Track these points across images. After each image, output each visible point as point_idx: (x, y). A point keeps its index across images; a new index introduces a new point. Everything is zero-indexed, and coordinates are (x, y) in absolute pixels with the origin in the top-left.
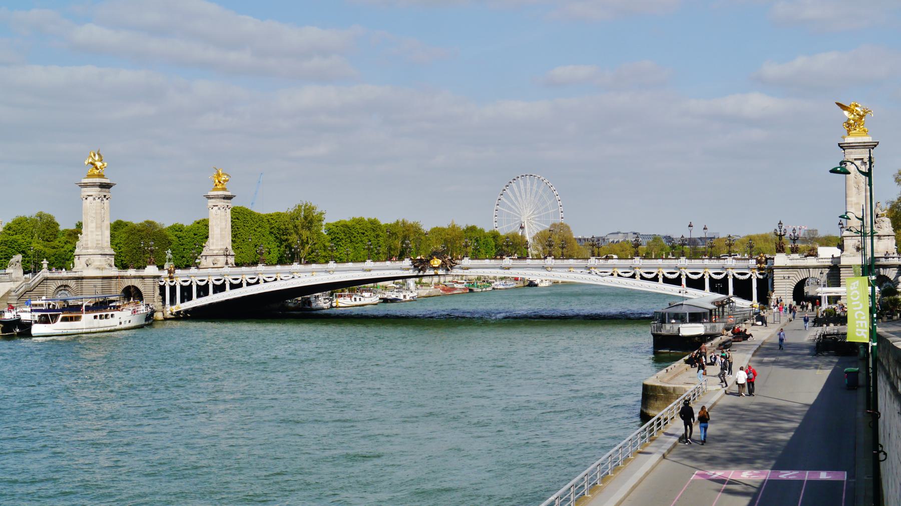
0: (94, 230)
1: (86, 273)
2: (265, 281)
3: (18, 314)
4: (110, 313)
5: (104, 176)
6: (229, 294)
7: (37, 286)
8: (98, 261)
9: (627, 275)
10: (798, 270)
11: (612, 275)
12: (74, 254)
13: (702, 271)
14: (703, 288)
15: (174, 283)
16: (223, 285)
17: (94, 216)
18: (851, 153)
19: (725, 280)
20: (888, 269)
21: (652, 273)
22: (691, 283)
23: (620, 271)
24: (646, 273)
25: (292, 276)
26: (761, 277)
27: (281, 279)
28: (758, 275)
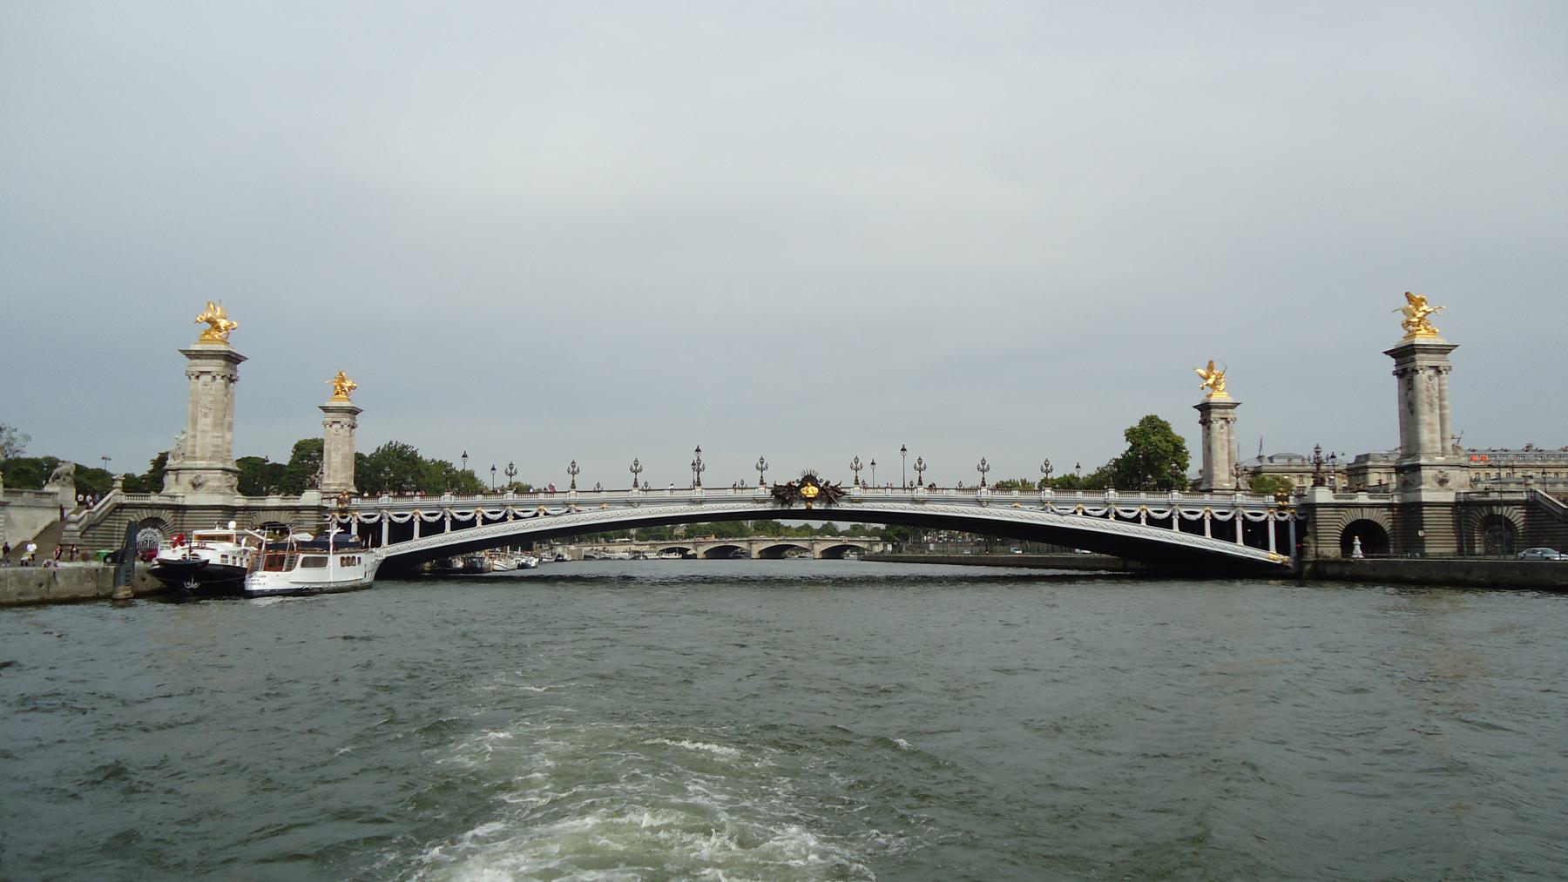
0: (210, 428)
1: (189, 500)
2: (516, 517)
3: (195, 551)
4: (357, 556)
7: (106, 518)
8: (215, 479)
9: (1098, 513)
10: (1347, 509)
11: (1075, 513)
12: (166, 467)
13: (1201, 511)
14: (1202, 533)
16: (442, 521)
17: (210, 406)
18: (1423, 359)
19: (1233, 521)
20: (1505, 508)
22: (1186, 526)
23: (1087, 509)
24: (1125, 511)
25: (566, 510)
27: (546, 514)
28: (1278, 517)
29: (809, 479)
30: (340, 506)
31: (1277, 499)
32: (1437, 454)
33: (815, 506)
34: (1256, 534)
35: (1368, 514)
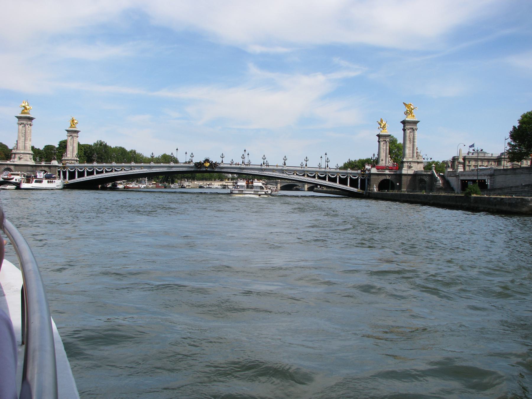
5: (29, 114)
6: (95, 176)
9: (301, 174)
11: (294, 174)
14: (336, 182)
15: (65, 170)
18: (408, 125)
19: (346, 178)
20: (424, 176)
21: (313, 174)
22: (331, 180)
24: (310, 174)
26: (363, 178)
27: (124, 170)
28: (362, 177)
29: (207, 161)
30: (63, 166)
31: (362, 171)
32: (410, 158)
33: (208, 169)
34: (354, 183)
35: (388, 177)
